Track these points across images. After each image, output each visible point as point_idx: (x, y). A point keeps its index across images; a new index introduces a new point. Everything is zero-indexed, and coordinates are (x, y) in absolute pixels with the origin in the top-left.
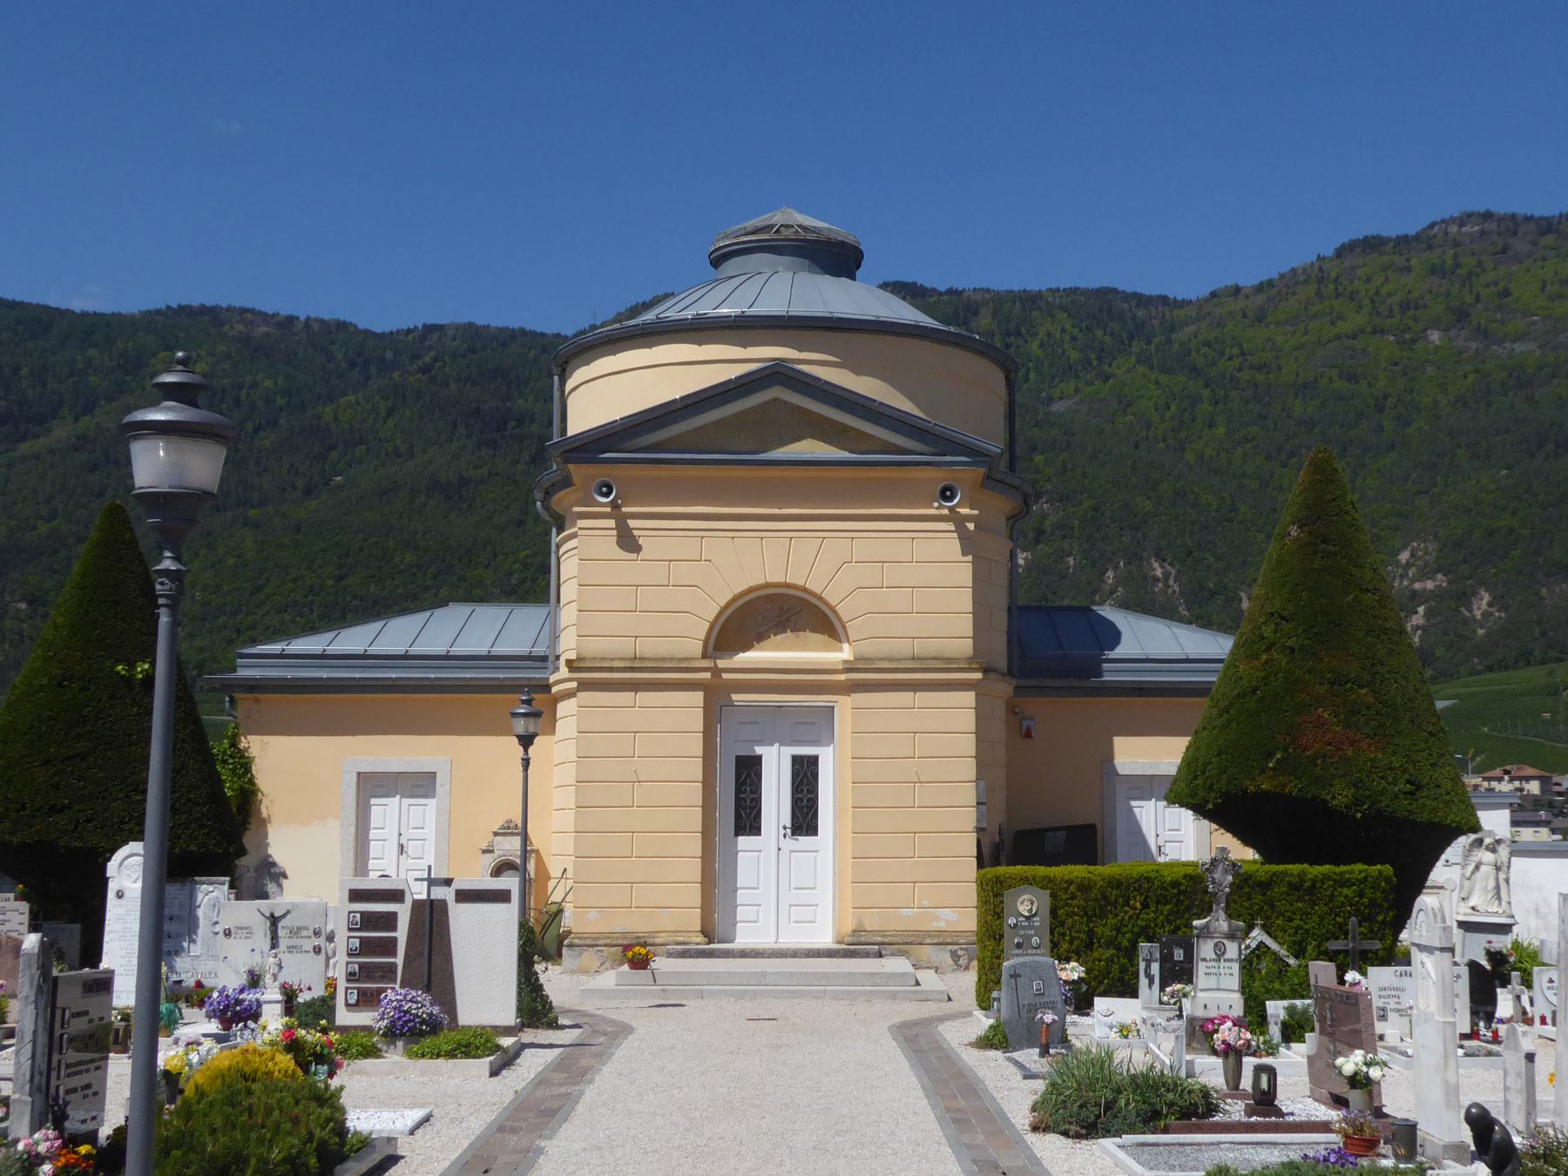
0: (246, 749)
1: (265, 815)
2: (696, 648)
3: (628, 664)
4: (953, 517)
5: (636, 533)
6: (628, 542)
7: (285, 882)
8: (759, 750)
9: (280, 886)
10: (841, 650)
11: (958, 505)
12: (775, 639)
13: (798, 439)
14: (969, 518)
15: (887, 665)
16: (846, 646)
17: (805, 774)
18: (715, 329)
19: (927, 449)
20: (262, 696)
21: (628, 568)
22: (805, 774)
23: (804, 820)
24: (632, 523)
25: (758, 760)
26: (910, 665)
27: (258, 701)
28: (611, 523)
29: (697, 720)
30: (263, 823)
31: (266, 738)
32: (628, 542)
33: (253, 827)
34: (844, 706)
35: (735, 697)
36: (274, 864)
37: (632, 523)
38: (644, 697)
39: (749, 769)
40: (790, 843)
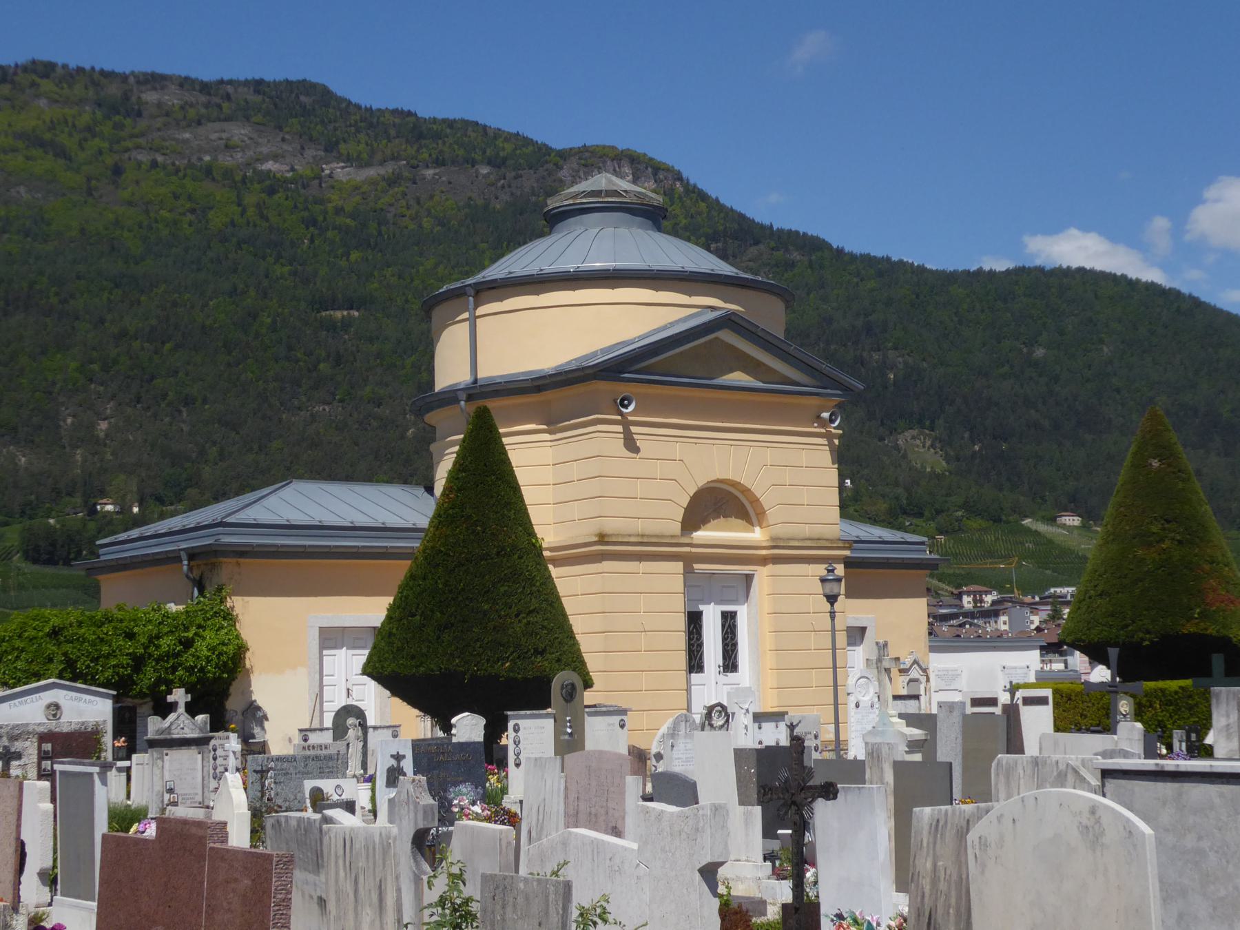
0: (233, 608)
1: (248, 666)
2: (676, 528)
3: (639, 539)
4: (829, 436)
5: (635, 436)
6: (631, 445)
7: (266, 724)
8: (701, 607)
9: (263, 728)
10: (753, 532)
11: (631, 414)
12: (714, 523)
13: (731, 371)
14: (835, 436)
15: (796, 544)
16: (757, 529)
17: (729, 621)
18: (645, 278)
19: (814, 382)
20: (241, 560)
21: (631, 464)
22: (729, 621)
23: (730, 663)
24: (633, 429)
25: (700, 614)
26: (808, 543)
27: (238, 564)
28: (620, 428)
29: (678, 583)
30: (248, 673)
31: (246, 598)
32: (631, 445)
33: (239, 676)
34: (763, 576)
35: (696, 566)
36: (259, 708)
37: (633, 429)
38: (643, 566)
39: (694, 621)
40: (723, 678)
